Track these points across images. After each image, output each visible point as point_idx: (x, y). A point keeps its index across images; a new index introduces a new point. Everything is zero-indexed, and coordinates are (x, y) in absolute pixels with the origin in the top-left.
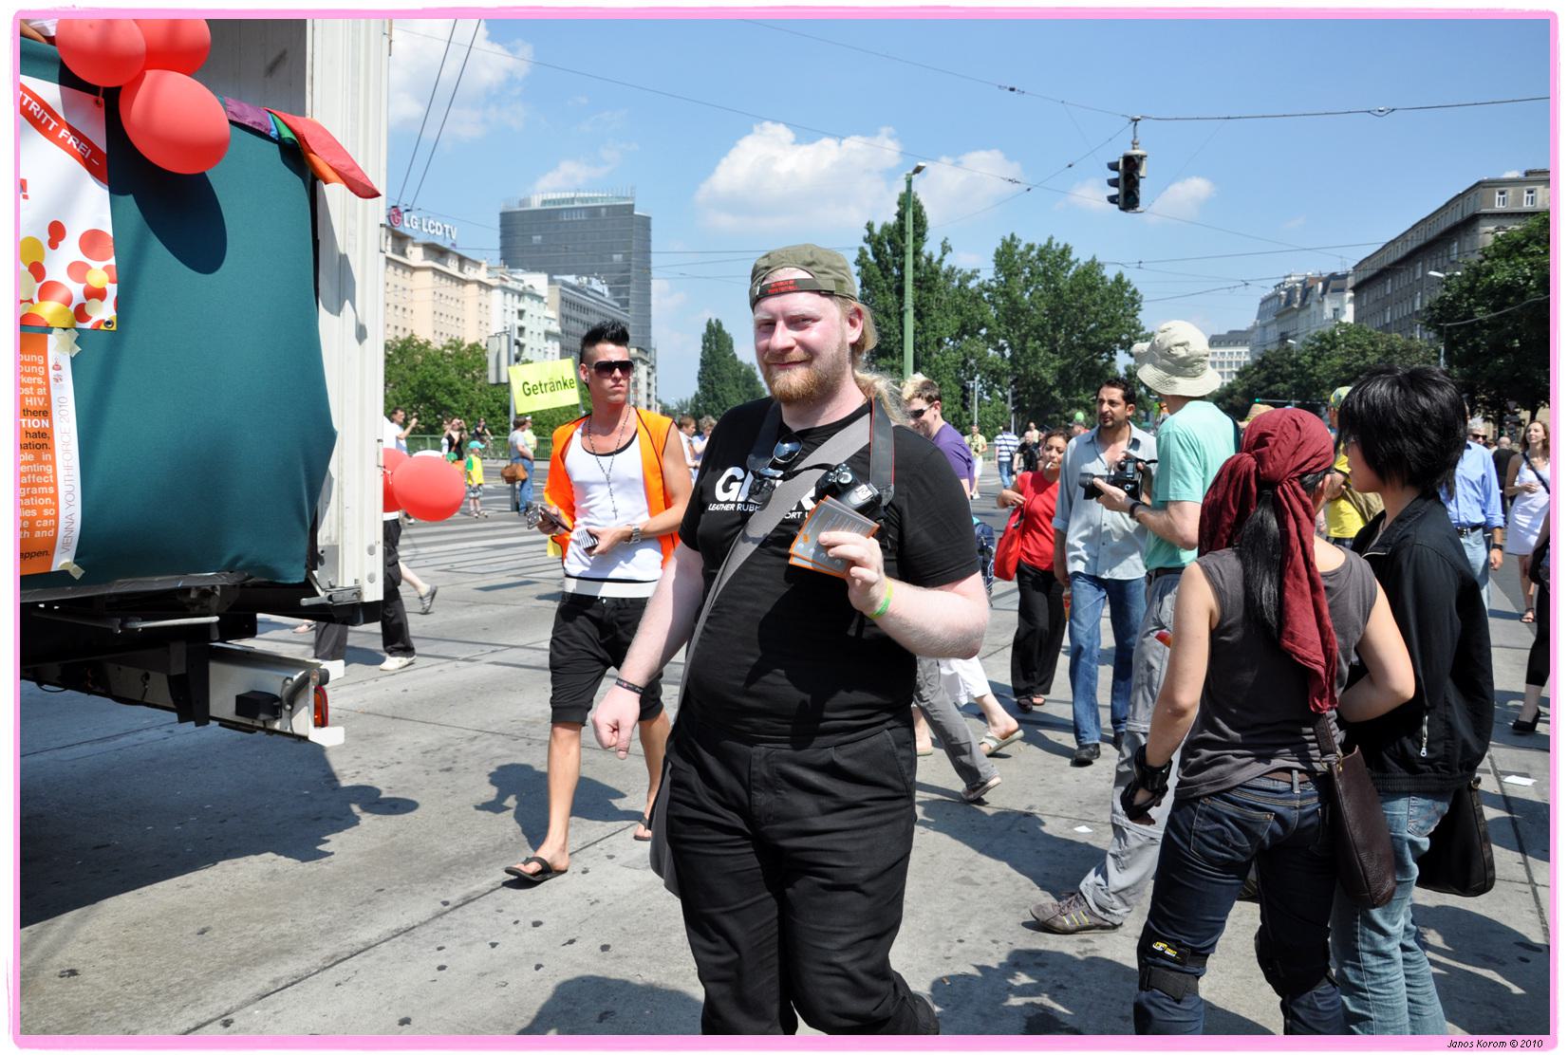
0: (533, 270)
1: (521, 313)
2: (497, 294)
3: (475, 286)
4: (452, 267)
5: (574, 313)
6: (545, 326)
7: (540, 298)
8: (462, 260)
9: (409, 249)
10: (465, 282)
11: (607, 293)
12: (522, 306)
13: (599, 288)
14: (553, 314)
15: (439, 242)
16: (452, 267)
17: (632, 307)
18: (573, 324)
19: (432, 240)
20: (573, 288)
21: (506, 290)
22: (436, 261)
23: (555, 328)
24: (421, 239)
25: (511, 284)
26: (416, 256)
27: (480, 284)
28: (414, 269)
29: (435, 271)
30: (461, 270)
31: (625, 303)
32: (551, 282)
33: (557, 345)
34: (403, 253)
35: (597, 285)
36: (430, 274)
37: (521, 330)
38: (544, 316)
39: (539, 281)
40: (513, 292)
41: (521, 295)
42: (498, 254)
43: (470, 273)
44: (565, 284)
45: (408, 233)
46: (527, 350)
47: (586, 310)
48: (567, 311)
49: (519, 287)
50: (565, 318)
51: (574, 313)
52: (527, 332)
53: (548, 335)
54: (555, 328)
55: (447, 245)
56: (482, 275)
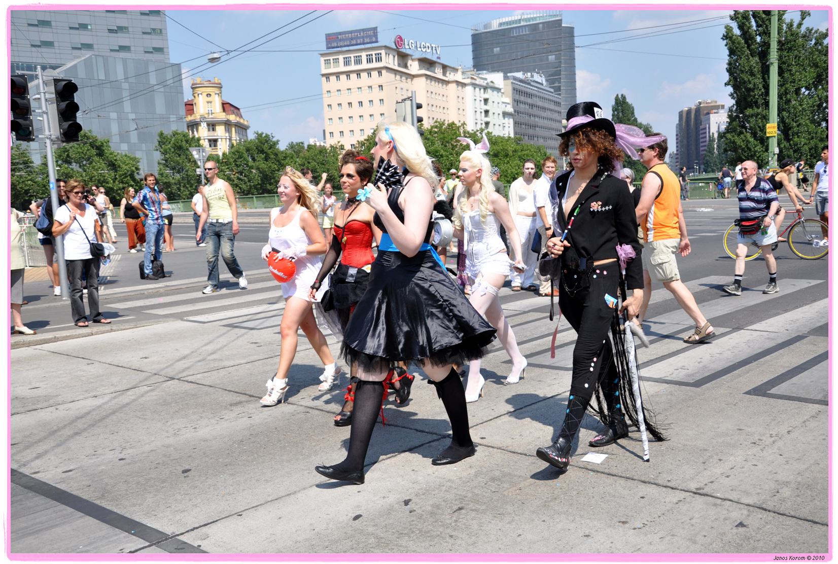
0: (494, 69)
1: (486, 101)
2: (469, 89)
3: (454, 85)
4: (438, 73)
5: (522, 98)
6: (503, 108)
7: (498, 90)
8: (445, 67)
9: (410, 62)
10: (447, 83)
11: (544, 82)
12: (486, 96)
13: (537, 78)
14: (508, 100)
15: (429, 57)
16: (438, 73)
17: (563, 92)
18: (522, 106)
19: (424, 56)
20: (521, 81)
21: (475, 86)
22: (428, 69)
23: (510, 109)
24: (418, 55)
25: (478, 82)
26: (414, 67)
27: (458, 83)
28: (413, 76)
29: (426, 75)
30: (444, 74)
31: (558, 89)
32: (506, 78)
33: (511, 121)
34: (406, 66)
35: (535, 74)
36: (424, 79)
37: (487, 112)
38: (502, 102)
39: (497, 78)
40: (480, 86)
41: (485, 88)
42: (470, 62)
43: (451, 76)
44: (515, 78)
45: (408, 52)
46: (491, 125)
47: (530, 95)
48: (517, 97)
49: (484, 83)
50: (516, 102)
51: (522, 98)
52: (490, 113)
53: (505, 114)
54: (510, 109)
55: (434, 59)
56: (459, 77)
